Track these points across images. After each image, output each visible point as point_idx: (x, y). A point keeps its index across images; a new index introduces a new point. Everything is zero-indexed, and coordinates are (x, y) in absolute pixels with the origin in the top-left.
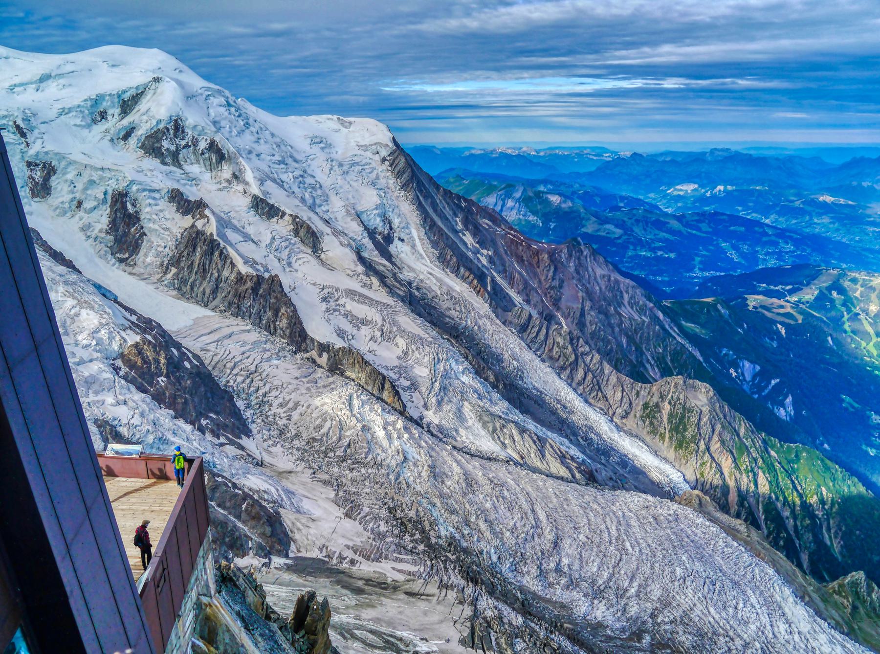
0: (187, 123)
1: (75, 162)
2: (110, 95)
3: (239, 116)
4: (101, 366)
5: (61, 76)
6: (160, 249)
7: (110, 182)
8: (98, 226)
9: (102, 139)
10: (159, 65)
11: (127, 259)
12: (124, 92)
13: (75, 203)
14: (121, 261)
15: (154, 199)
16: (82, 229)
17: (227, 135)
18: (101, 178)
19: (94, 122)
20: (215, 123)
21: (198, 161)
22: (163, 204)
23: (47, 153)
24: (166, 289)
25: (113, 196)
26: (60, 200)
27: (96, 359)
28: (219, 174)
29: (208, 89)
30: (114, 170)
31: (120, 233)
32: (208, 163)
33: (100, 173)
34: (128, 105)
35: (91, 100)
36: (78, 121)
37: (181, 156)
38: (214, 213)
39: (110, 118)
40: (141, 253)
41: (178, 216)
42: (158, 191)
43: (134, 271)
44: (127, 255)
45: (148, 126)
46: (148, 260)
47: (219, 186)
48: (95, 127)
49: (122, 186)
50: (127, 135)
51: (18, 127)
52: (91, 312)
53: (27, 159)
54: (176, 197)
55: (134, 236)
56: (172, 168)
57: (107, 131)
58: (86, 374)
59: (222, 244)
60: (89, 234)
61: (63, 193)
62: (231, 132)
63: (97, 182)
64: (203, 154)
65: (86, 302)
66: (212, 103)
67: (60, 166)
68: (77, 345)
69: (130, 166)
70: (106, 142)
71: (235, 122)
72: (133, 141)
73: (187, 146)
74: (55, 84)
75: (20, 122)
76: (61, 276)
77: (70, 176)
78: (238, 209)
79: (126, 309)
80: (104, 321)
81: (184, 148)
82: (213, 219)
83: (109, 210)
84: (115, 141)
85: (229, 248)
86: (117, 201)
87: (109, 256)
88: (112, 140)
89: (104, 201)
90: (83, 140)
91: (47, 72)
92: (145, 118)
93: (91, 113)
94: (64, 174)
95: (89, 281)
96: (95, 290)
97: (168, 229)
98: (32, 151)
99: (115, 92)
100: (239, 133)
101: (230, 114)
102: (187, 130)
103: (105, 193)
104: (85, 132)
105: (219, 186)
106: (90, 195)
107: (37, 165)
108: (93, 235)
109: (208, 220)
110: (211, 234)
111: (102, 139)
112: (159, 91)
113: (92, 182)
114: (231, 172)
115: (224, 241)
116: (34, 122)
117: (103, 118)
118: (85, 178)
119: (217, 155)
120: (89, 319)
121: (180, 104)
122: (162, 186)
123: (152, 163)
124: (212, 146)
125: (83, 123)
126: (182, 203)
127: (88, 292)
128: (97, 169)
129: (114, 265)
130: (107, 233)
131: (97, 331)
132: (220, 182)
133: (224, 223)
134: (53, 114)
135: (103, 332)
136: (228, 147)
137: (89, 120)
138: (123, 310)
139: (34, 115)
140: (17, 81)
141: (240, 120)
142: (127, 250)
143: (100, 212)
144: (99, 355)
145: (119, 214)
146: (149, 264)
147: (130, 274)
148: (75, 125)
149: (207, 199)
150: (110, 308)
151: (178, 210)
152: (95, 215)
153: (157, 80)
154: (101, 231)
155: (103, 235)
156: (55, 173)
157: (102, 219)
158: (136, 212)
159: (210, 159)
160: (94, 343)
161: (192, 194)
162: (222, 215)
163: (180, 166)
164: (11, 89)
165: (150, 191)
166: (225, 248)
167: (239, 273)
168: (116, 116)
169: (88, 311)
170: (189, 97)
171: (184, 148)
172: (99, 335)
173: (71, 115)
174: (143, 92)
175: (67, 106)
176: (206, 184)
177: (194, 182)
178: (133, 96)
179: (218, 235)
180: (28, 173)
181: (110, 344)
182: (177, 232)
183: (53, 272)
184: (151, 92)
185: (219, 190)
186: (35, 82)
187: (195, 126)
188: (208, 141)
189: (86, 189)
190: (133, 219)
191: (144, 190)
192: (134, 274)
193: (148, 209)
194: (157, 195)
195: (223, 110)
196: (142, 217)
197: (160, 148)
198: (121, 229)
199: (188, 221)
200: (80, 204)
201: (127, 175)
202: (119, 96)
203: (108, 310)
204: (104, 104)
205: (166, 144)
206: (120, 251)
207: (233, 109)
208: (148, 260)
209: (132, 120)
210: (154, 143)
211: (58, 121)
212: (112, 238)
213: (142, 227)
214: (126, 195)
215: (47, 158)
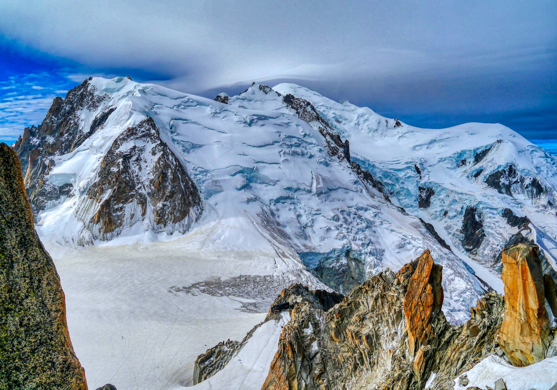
0: (518, 167)
1: (446, 189)
2: (469, 151)
3: (554, 164)
4: (466, 316)
5: (441, 140)
6: (494, 246)
7: (466, 201)
8: (456, 228)
9: (462, 176)
10: (500, 133)
11: (471, 250)
12: (478, 149)
13: (443, 212)
14: (468, 250)
15: (493, 214)
16: (447, 228)
17: (545, 176)
18: (460, 199)
19: (458, 166)
20: (537, 168)
21: (523, 192)
22: (499, 218)
23: (430, 183)
24: (497, 273)
25: (467, 210)
26: (435, 210)
27: (462, 310)
28: (538, 201)
29: (532, 147)
30: (469, 195)
31: (469, 233)
32: (530, 194)
33: (460, 196)
34: (479, 156)
35: (458, 153)
36: (449, 166)
37: (512, 188)
38: (535, 227)
39: (467, 164)
40: (481, 247)
41: (508, 226)
42: (496, 209)
43: (475, 258)
44: (471, 247)
45: (492, 169)
46: (486, 252)
47: (537, 209)
48: (458, 169)
49: (473, 204)
50: (478, 174)
51: (417, 168)
52: (461, 280)
53: (419, 185)
54: (508, 214)
55: (477, 236)
56: (505, 195)
57: (465, 171)
58: (457, 319)
59: (540, 248)
60: (450, 231)
61: (437, 206)
62: (548, 174)
63: (458, 201)
64: (527, 187)
65: (459, 273)
66: (535, 155)
67: (437, 190)
68: (451, 298)
69: (479, 193)
70: (464, 177)
71: (550, 168)
72: (481, 178)
73: (516, 182)
74: (438, 145)
75: (418, 166)
76: (446, 254)
77: (442, 197)
78: (551, 226)
79: (482, 281)
80: (469, 287)
81: (514, 183)
82: (534, 231)
83: (463, 218)
84: (470, 177)
85: (545, 252)
86: (469, 213)
87: (461, 247)
88: (468, 177)
89: (461, 213)
90: (451, 177)
91: (434, 138)
92: (490, 164)
93: (457, 161)
94: (439, 195)
95: (460, 260)
96: (465, 267)
97: (501, 234)
98: (422, 182)
99: (472, 149)
100: (553, 175)
101: (547, 162)
102: (517, 172)
103: (462, 208)
104: (452, 172)
105: (537, 209)
106: (453, 208)
107: (424, 189)
108: (452, 232)
109: (531, 231)
110: (533, 241)
111: (462, 176)
112: (500, 148)
113: (455, 201)
114: (547, 201)
115: (541, 246)
116: (425, 166)
117: (463, 164)
118: (451, 199)
119: (537, 188)
120: (460, 284)
121: (514, 156)
122: (499, 206)
123: (493, 192)
124: (535, 183)
125: (452, 167)
126: (512, 218)
127: (460, 267)
128: (458, 193)
129: (463, 252)
130: (461, 232)
131: (464, 292)
132: (538, 207)
133: (541, 234)
134: (435, 161)
135: (468, 293)
136: (545, 183)
137: (455, 165)
138: (480, 282)
139: (426, 162)
140: (418, 143)
141: (554, 166)
142: (472, 244)
143: (458, 219)
144: (464, 308)
145: (469, 221)
146: (486, 255)
147: (473, 259)
148: (447, 168)
149: (529, 217)
150: (473, 279)
151: (508, 223)
152: (455, 220)
153: (499, 141)
154: (457, 230)
155: (458, 233)
156: (433, 194)
157: (458, 224)
158: (481, 221)
159: (532, 191)
160: (462, 299)
161: (519, 213)
162: (540, 228)
163: (511, 195)
164: (414, 148)
165: (491, 209)
166: (542, 251)
167: (552, 270)
168: (472, 163)
169: (459, 278)
170: (520, 151)
171: (514, 183)
172: (464, 295)
173: (445, 162)
174: (490, 149)
175: (444, 157)
176: (526, 206)
177: (520, 205)
178: (483, 151)
179: (537, 241)
180: (419, 193)
181: (471, 302)
182: (507, 237)
183: (442, 251)
184: (495, 149)
185: (538, 212)
186: (427, 144)
187: (524, 170)
188: (532, 180)
189: (450, 204)
190: (478, 225)
191: (487, 208)
192: (476, 260)
193: (488, 220)
194: (495, 212)
195: (542, 160)
196: (484, 225)
197: (499, 183)
198: (470, 230)
199: (515, 230)
200: (446, 213)
201: (477, 198)
202: (475, 151)
203: (472, 281)
204: (465, 156)
205: (502, 180)
206: (468, 244)
207: (549, 160)
208: (486, 252)
209: (481, 165)
210: (494, 180)
211: (438, 165)
212: (463, 235)
213: (483, 231)
214: (475, 210)
215: (430, 186)
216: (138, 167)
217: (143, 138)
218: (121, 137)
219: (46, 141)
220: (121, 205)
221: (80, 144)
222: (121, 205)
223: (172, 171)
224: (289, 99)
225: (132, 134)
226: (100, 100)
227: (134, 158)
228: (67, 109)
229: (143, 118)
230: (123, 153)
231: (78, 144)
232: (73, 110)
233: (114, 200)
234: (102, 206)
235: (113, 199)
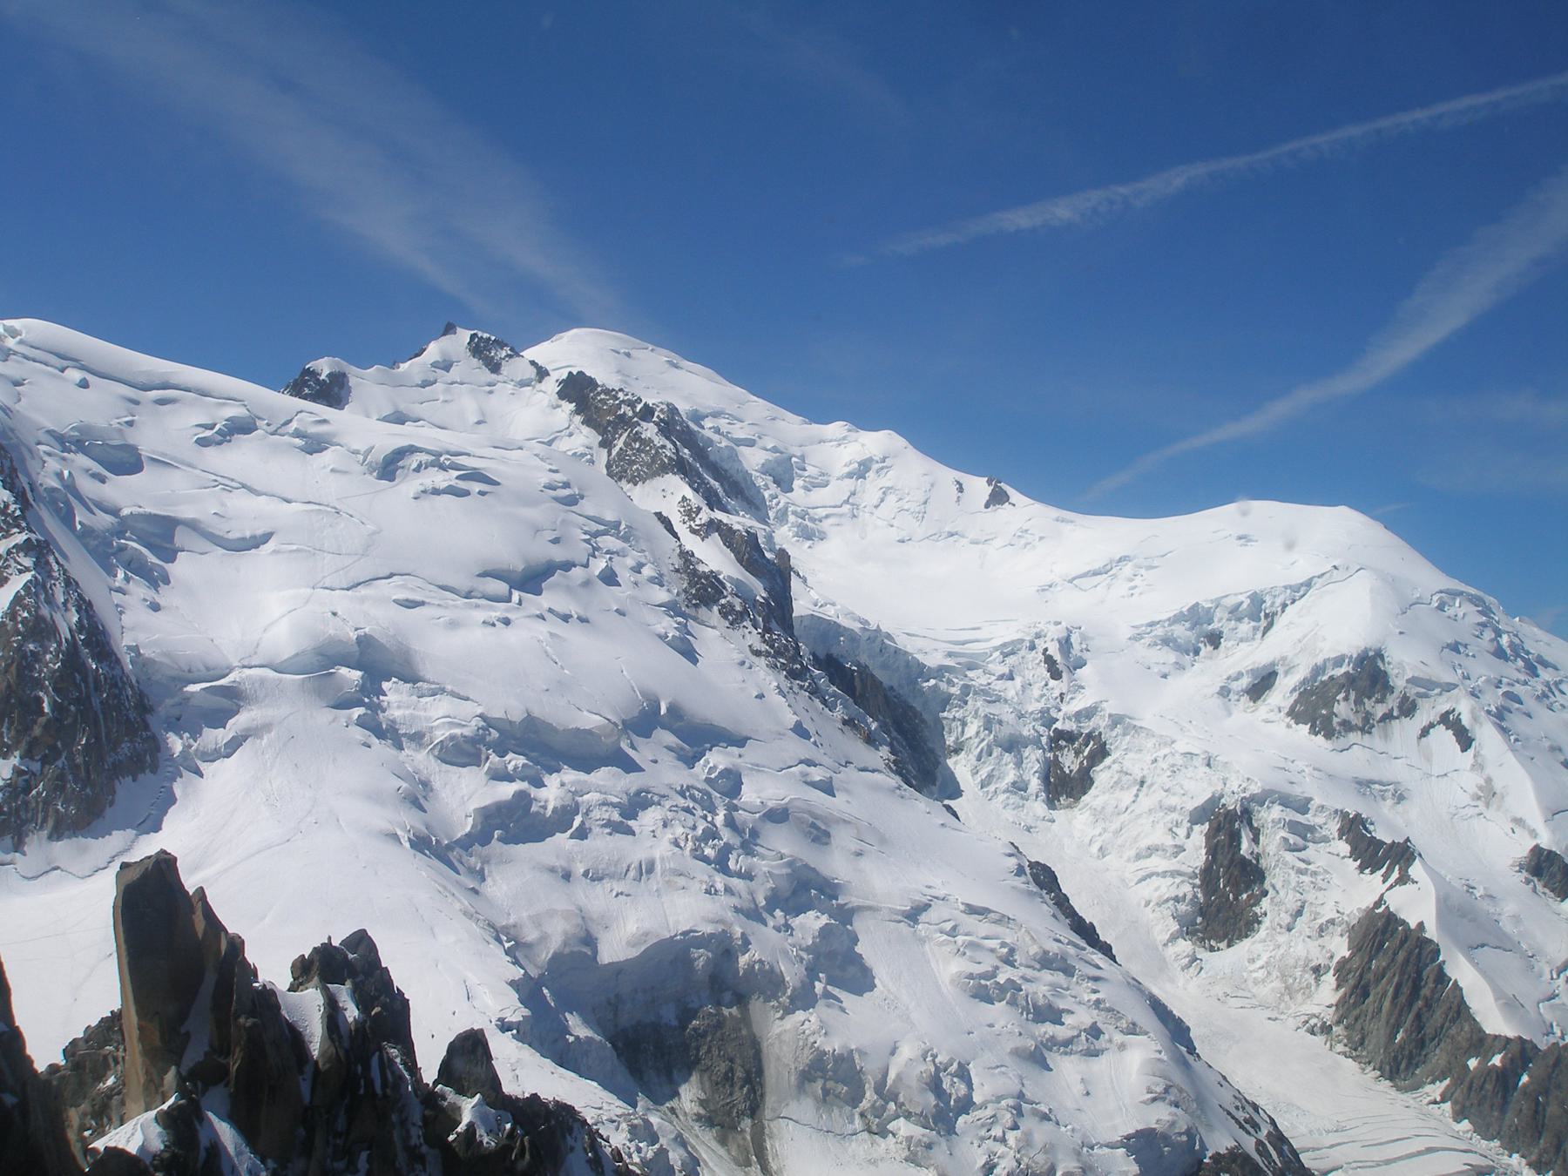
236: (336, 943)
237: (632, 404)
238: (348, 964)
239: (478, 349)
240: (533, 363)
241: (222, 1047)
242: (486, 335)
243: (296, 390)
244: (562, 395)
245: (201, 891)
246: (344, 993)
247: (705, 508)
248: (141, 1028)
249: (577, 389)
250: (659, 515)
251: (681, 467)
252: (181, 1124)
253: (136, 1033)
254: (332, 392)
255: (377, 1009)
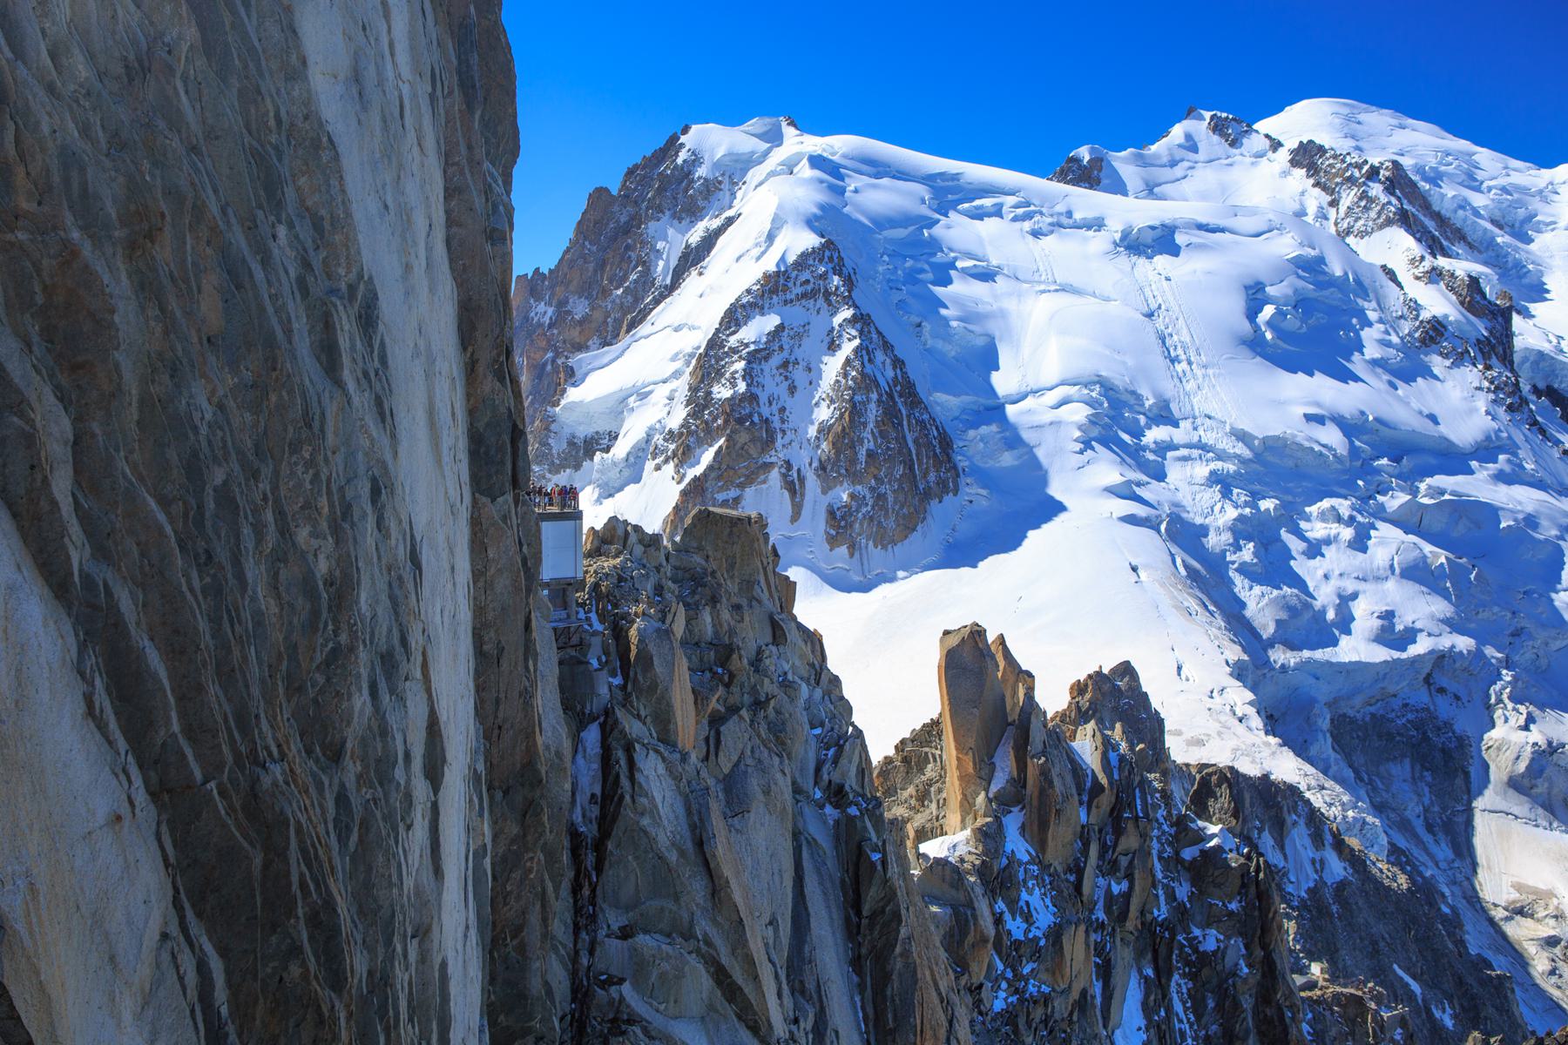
216: (786, 384)
217: (803, 302)
218: (744, 300)
219: (569, 313)
220: (732, 493)
221: (641, 322)
222: (732, 493)
223: (880, 395)
224: (1307, 156)
225: (774, 291)
226: (711, 189)
227: (776, 360)
228: (623, 219)
229: (810, 240)
230: (747, 345)
231: (633, 325)
232: (635, 222)
233: (719, 478)
234: (684, 493)
235: (713, 475)
236: (1106, 671)
237: (1359, 166)
238: (1115, 697)
239: (1218, 127)
240: (1267, 136)
241: (1019, 782)
242: (1224, 115)
243: (1062, 177)
244: (1294, 163)
245: (1001, 640)
246: (1117, 733)
247: (1428, 256)
248: (958, 759)
249: (1307, 156)
250: (1384, 267)
251: (1404, 220)
252: (989, 837)
253: (954, 763)
254: (1089, 176)
255: (1141, 746)
